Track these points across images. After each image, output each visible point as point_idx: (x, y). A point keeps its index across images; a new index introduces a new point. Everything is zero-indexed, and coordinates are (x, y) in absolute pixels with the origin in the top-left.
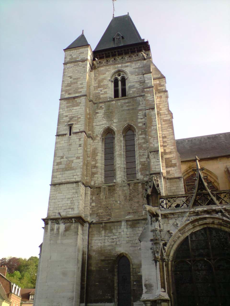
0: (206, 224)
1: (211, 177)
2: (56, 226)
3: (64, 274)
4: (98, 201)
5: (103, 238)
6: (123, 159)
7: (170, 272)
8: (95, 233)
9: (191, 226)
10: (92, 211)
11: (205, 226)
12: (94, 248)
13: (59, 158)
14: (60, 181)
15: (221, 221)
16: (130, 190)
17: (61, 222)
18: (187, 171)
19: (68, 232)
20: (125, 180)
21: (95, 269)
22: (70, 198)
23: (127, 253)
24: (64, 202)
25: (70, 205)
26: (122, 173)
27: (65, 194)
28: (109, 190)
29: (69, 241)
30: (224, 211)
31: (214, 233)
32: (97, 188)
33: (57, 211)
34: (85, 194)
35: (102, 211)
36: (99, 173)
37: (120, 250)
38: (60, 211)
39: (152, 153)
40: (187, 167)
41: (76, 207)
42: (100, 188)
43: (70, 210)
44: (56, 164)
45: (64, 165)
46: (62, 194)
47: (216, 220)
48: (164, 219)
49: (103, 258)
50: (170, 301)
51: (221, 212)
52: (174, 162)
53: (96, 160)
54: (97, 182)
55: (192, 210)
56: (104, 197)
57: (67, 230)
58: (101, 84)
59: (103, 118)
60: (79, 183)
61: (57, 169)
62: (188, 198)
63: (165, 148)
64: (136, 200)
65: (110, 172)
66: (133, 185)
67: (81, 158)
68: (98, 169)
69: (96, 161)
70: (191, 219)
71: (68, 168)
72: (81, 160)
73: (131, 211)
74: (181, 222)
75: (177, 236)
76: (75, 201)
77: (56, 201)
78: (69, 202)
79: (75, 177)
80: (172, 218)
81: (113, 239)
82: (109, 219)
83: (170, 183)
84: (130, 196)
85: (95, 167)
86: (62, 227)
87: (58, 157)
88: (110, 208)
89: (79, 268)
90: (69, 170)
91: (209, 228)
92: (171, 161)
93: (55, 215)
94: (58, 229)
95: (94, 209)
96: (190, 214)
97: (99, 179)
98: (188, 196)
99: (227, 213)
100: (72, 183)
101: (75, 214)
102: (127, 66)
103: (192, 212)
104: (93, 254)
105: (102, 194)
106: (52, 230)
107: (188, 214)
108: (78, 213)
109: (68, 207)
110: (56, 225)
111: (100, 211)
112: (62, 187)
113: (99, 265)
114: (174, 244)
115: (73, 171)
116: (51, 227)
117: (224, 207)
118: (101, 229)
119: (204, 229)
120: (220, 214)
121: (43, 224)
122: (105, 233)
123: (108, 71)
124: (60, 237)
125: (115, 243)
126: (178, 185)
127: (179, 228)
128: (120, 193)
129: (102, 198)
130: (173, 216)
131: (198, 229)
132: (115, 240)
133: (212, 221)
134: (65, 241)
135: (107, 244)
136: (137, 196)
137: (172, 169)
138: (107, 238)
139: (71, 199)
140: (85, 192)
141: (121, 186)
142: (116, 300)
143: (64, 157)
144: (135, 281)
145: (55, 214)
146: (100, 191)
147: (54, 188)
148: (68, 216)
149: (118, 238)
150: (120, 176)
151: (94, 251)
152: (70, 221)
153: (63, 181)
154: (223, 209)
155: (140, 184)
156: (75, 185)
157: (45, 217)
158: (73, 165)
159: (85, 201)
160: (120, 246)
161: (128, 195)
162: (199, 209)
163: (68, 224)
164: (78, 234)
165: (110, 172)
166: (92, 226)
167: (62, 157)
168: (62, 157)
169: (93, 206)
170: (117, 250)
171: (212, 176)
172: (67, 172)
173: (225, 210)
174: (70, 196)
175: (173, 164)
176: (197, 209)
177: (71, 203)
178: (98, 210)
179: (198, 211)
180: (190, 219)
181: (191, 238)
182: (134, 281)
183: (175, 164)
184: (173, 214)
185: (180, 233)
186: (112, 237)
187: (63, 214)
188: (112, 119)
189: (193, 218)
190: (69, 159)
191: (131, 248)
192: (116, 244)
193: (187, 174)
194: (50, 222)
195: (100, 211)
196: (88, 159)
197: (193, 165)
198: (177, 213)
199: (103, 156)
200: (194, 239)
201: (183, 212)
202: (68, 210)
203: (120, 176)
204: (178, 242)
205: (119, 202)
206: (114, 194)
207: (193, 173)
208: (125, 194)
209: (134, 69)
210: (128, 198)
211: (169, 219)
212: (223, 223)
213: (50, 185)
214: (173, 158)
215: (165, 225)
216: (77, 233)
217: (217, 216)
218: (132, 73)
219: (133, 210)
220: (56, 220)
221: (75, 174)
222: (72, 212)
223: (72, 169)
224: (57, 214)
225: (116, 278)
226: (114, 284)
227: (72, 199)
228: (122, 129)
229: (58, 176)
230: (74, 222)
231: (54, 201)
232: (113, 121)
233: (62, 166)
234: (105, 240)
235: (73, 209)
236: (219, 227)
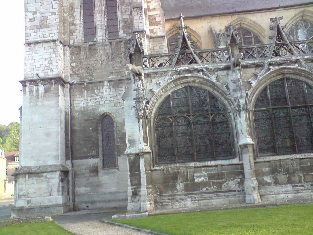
0: (187, 82)
1: (194, 37)
2: (35, 88)
3: (48, 135)
4: (79, 61)
5: (86, 98)
6: (104, 16)
7: (152, 128)
8: (77, 93)
9: (173, 85)
10: (73, 72)
11: (187, 85)
12: (77, 108)
13: (31, 14)
14: (34, 40)
15: (202, 80)
16: (112, 49)
17: (39, 83)
18: (170, 30)
19: (48, 94)
20: (107, 39)
21: (78, 129)
22: (47, 59)
23: (110, 112)
24: (41, 63)
25: (48, 65)
26: (103, 31)
27: (41, 54)
28: (90, 49)
29: (51, 102)
30: (205, 70)
31: (194, 90)
32: (76, 47)
33: (35, 73)
34: (64, 54)
35: (83, 71)
36: (77, 31)
37: (104, 109)
38: (38, 72)
39: (135, 10)
40: (171, 26)
41: (54, 67)
42: (79, 47)
43: (49, 71)
44: (28, 20)
45: (38, 22)
46: (39, 54)
47: (197, 79)
48: (147, 78)
49: (86, 118)
50: (152, 153)
51: (202, 71)
52: (157, 19)
53: (74, 16)
54: (76, 41)
55: (175, 69)
56: (85, 57)
57: (46, 91)
60: (57, 42)
61: (30, 26)
62: (170, 57)
63: (149, 4)
64: (118, 60)
65: (90, 30)
66: (115, 44)
67: (57, 13)
68: (76, 26)
69: (74, 17)
70: (174, 78)
71: (43, 25)
72: (57, 16)
73: (114, 71)
74: (164, 81)
75: (159, 95)
76: (53, 62)
77: (33, 61)
78: (47, 62)
79: (51, 35)
80: (154, 78)
81: (96, 99)
82: (91, 79)
83: (154, 42)
84: (112, 56)
85: (73, 24)
86: (42, 88)
87: (30, 12)
88: (91, 68)
89: (62, 128)
90: (44, 28)
91: (190, 87)
92: (155, 19)
93: (33, 77)
94: (37, 91)
95: (74, 70)
96: (172, 73)
97: (78, 37)
98: (171, 55)
99: (208, 72)
100: (49, 42)
101: (54, 75)
103: (174, 72)
104: (76, 114)
105: (82, 53)
106: (31, 92)
107: (170, 73)
108: (58, 74)
109: (46, 68)
110: (35, 87)
111: (80, 71)
112: (37, 46)
113: (83, 125)
114: (156, 103)
115: (50, 29)
116: (30, 89)
117: (206, 66)
118: (83, 90)
119: (186, 87)
120: (201, 73)
121: (20, 86)
122: (87, 93)
124: (40, 99)
125: (98, 103)
126: (162, 45)
127: (161, 87)
128: (102, 52)
129: (82, 58)
130: (155, 75)
131: (180, 87)
132: (98, 100)
133: (193, 80)
134: (46, 103)
135: (90, 104)
136: (119, 55)
137: (156, 27)
138: (89, 98)
139: (49, 60)
140: (64, 52)
141: (102, 45)
142: (101, 156)
143: (37, 13)
144: (119, 138)
145: (32, 75)
146: (80, 50)
147: (28, 47)
148: (47, 77)
149: (101, 98)
150: (101, 34)
151: (77, 111)
152: (49, 82)
153: (38, 39)
154: (204, 68)
155: (123, 43)
156: (52, 44)
157: (22, 79)
158: (48, 22)
159: (64, 62)
160: (103, 105)
161: (110, 54)
162: (182, 68)
163: (48, 85)
164: (59, 96)
165: (90, 30)
166: (73, 86)
167: (35, 13)
168: (35, 13)
169: (73, 67)
170: (100, 110)
171: (195, 36)
172: (42, 30)
173: (207, 69)
174: (47, 57)
175: (157, 22)
176: (179, 68)
177: (49, 64)
178: (78, 70)
179: (180, 70)
180: (172, 78)
181: (173, 96)
182: (117, 138)
183: (159, 22)
184: (156, 73)
185: (162, 92)
186: (94, 98)
187: (42, 75)
189: (175, 77)
190: (44, 15)
191: (114, 108)
192: (99, 104)
193: (171, 33)
194: (28, 84)
196: (65, 15)
197: (177, 24)
198: (161, 72)
199: (82, 11)
200: (175, 97)
201: (166, 71)
202: (47, 71)
203: (101, 34)
204: (160, 100)
205: (100, 62)
206: (95, 53)
207: (177, 32)
208: (107, 53)
210: (110, 58)
211: (152, 78)
212: (203, 81)
213: (24, 44)
214: (156, 16)
215: (148, 84)
216: (58, 94)
217: (198, 75)
220: (34, 82)
221: (52, 32)
222: (51, 73)
223: (47, 26)
224: (35, 76)
225: (100, 136)
226: (98, 142)
227: (50, 59)
229: (32, 34)
230: (54, 83)
231: (30, 61)
233: (36, 23)
234: (87, 100)
235: (52, 70)
236: (200, 85)
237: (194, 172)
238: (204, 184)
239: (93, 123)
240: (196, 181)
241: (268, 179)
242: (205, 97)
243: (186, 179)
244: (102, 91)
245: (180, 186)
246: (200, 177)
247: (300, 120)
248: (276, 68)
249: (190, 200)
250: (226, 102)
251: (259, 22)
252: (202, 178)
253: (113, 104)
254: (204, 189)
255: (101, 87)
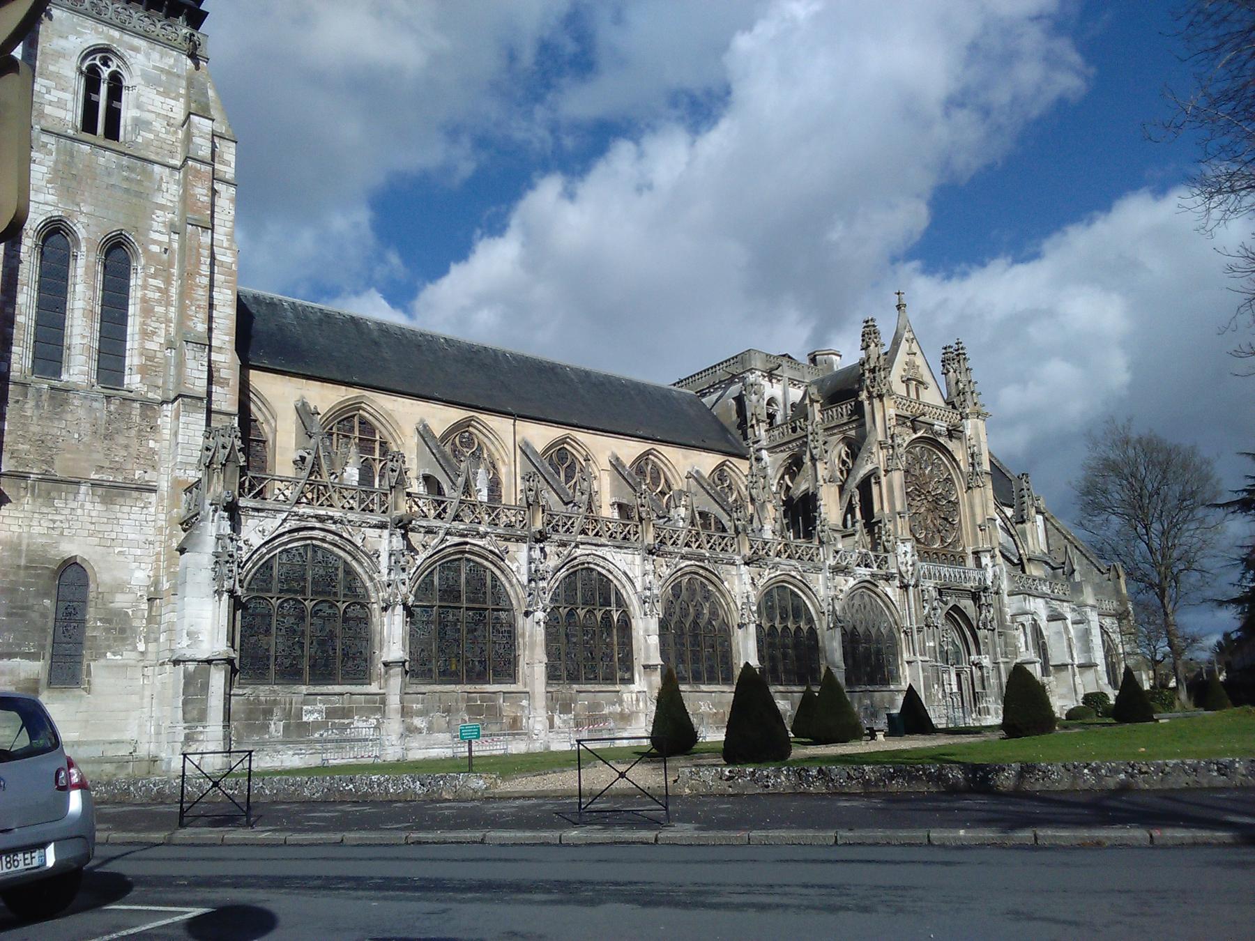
1: (260, 409)
28: (52, 398)
31: (320, 553)
35: (26, 447)
37: (69, 549)
58: (51, 68)
59: (48, 182)
73: (107, 464)
84: (107, 429)
102: (136, 49)
111: (21, 446)
113: (12, 577)
123: (79, 34)
128: (81, 413)
129: (29, 414)
132: (58, 523)
135: (36, 530)
138: (36, 515)
142: (48, 656)
144: (100, 620)
146: (26, 396)
155: (137, 405)
160: (71, 538)
170: (61, 548)
171: (264, 409)
182: (95, 620)
186: (50, 517)
188: (78, 200)
195: (21, 446)
205: (76, 436)
206: (63, 411)
209: (155, 68)
218: (150, 81)
219: (111, 462)
228: (99, 237)
232: (78, 205)
237: (305, 703)
238: (317, 726)
239: (38, 576)
240: (305, 719)
241: (418, 722)
242: (337, 569)
243: (287, 715)
244: (74, 505)
245: (276, 728)
246: (311, 712)
247: (476, 630)
248: (457, 540)
249: (291, 753)
250: (368, 584)
251: (397, 416)
252: (316, 715)
253: (95, 540)
254: (317, 735)
255: (71, 496)
